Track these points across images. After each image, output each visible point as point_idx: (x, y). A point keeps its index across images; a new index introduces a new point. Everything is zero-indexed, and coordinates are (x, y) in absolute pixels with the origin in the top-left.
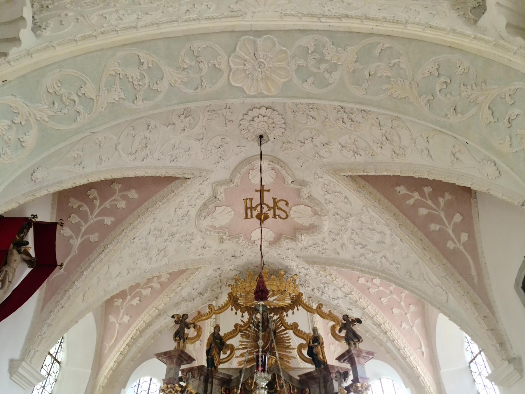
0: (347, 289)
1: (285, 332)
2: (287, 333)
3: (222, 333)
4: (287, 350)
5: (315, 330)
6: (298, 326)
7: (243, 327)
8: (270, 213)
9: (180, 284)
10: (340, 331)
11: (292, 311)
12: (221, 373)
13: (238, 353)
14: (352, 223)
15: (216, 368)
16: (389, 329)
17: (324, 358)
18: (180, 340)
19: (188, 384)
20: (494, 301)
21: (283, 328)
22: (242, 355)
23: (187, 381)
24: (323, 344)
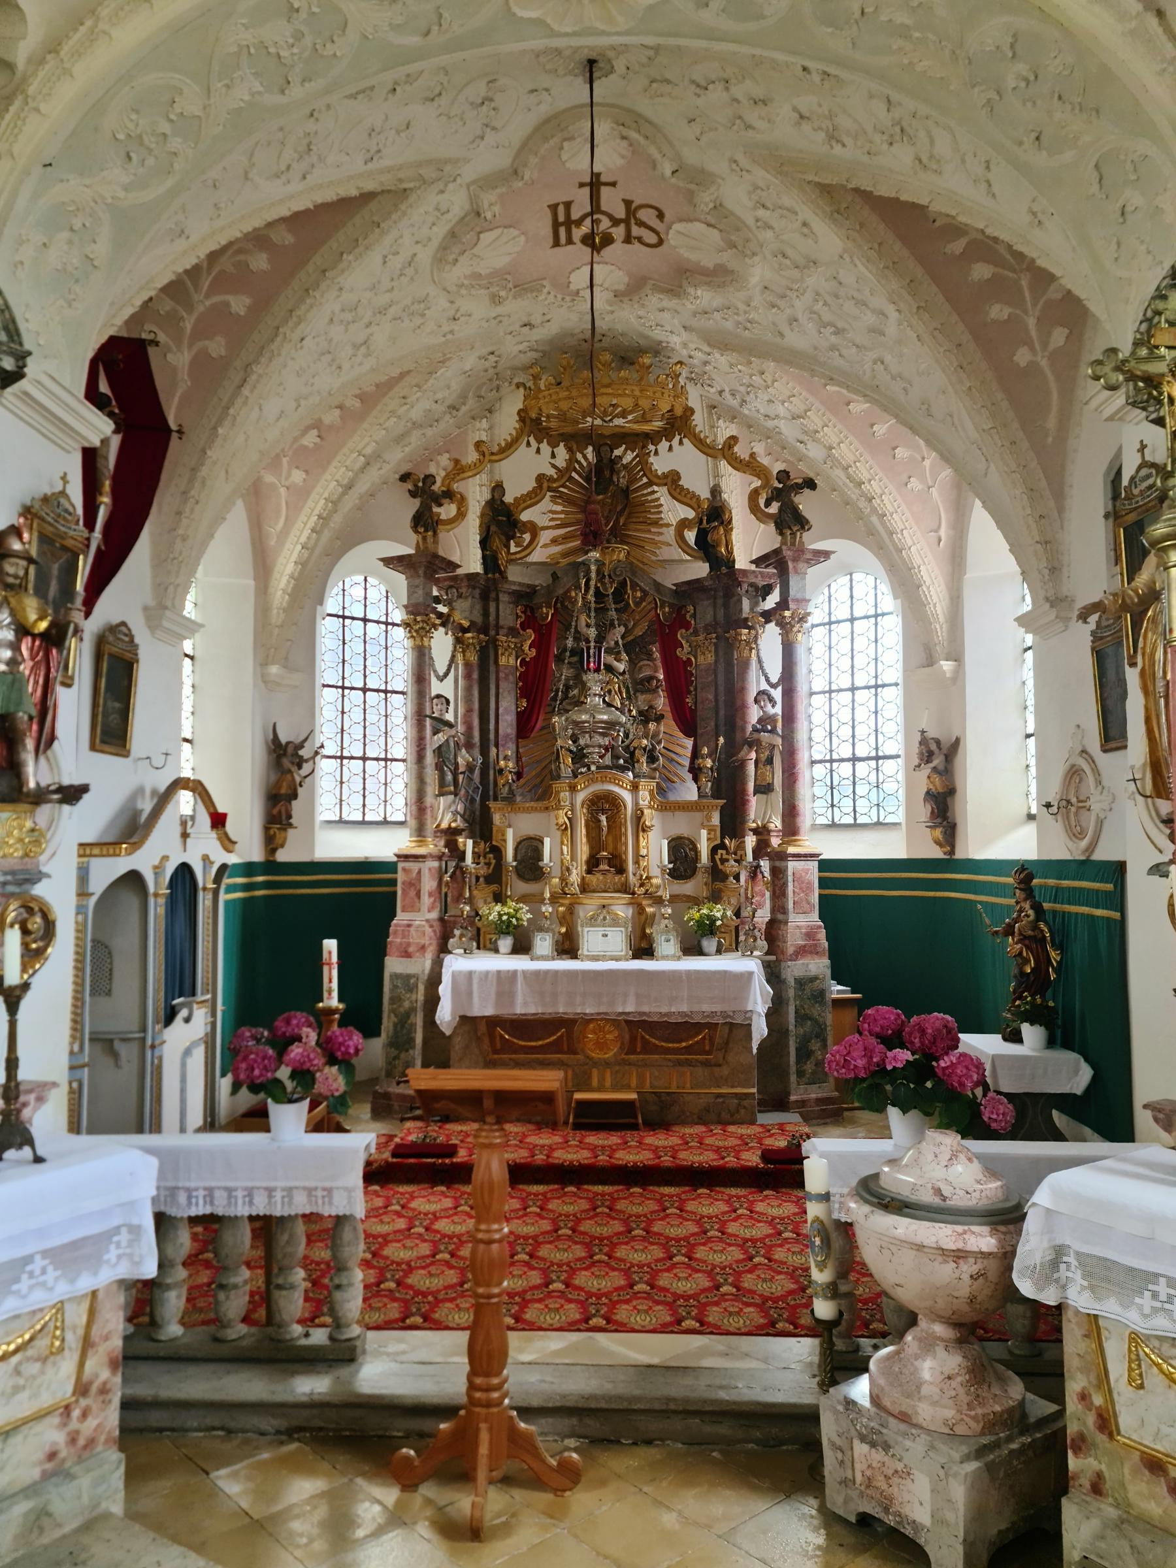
0: (797, 405)
1: (649, 490)
3: (509, 498)
4: (653, 530)
5: (716, 491)
6: (679, 478)
7: (555, 481)
8: (618, 232)
9: (404, 398)
10: (768, 504)
11: (668, 444)
12: (514, 583)
13: (545, 537)
14: (815, 280)
15: (503, 575)
16: (879, 491)
17: (730, 552)
18: (426, 531)
19: (452, 609)
20: (1071, 486)
21: (645, 480)
22: (554, 541)
23: (448, 603)
24: (730, 522)
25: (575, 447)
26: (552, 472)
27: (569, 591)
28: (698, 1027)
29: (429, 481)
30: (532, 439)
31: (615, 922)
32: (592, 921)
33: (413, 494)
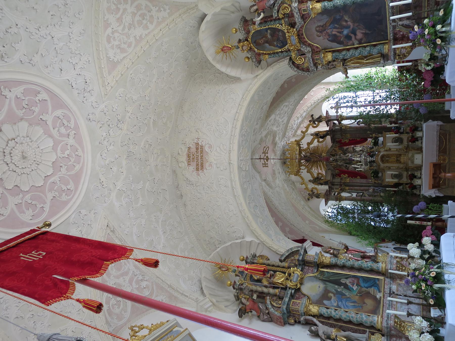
0: (296, 119)
1: (310, 148)
2: (311, 148)
5: (312, 135)
7: (308, 169)
8: (267, 155)
12: (331, 178)
13: (320, 171)
14: (277, 118)
16: (314, 101)
17: (325, 131)
18: (320, 195)
21: (308, 150)
22: (321, 169)
25: (301, 165)
26: (306, 170)
27: (332, 166)
28: (440, 137)
29: (310, 194)
30: (300, 174)
31: (413, 156)
32: (413, 162)
33: (312, 198)
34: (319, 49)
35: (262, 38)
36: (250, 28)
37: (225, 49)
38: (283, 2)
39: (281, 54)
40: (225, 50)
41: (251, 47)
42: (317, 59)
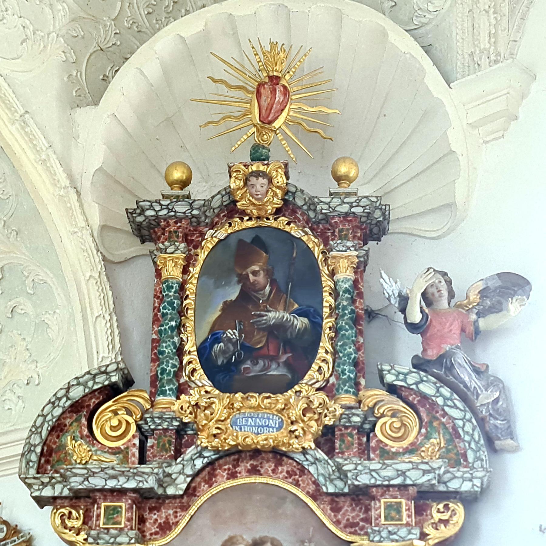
34: (156, 533)
35: (273, 283)
36: (349, 244)
37: (279, 97)
38: (435, 424)
39: (174, 343)
40: (274, 92)
41: (242, 219)
42: (112, 512)
